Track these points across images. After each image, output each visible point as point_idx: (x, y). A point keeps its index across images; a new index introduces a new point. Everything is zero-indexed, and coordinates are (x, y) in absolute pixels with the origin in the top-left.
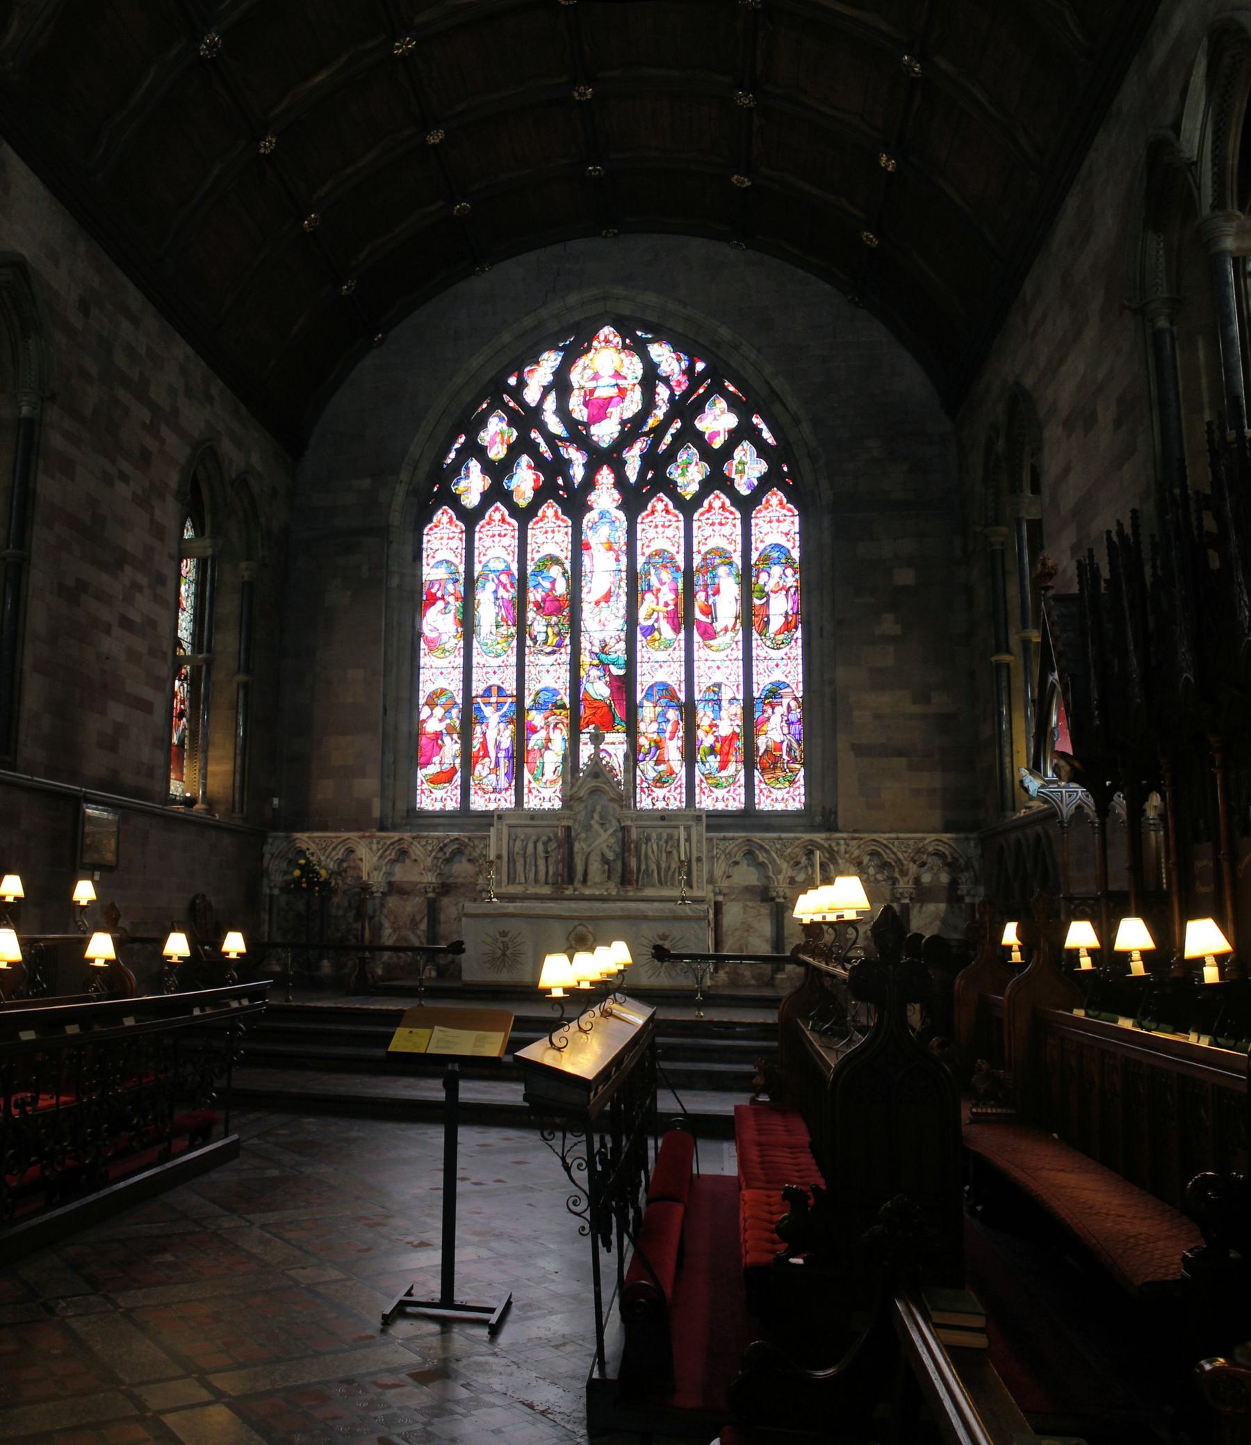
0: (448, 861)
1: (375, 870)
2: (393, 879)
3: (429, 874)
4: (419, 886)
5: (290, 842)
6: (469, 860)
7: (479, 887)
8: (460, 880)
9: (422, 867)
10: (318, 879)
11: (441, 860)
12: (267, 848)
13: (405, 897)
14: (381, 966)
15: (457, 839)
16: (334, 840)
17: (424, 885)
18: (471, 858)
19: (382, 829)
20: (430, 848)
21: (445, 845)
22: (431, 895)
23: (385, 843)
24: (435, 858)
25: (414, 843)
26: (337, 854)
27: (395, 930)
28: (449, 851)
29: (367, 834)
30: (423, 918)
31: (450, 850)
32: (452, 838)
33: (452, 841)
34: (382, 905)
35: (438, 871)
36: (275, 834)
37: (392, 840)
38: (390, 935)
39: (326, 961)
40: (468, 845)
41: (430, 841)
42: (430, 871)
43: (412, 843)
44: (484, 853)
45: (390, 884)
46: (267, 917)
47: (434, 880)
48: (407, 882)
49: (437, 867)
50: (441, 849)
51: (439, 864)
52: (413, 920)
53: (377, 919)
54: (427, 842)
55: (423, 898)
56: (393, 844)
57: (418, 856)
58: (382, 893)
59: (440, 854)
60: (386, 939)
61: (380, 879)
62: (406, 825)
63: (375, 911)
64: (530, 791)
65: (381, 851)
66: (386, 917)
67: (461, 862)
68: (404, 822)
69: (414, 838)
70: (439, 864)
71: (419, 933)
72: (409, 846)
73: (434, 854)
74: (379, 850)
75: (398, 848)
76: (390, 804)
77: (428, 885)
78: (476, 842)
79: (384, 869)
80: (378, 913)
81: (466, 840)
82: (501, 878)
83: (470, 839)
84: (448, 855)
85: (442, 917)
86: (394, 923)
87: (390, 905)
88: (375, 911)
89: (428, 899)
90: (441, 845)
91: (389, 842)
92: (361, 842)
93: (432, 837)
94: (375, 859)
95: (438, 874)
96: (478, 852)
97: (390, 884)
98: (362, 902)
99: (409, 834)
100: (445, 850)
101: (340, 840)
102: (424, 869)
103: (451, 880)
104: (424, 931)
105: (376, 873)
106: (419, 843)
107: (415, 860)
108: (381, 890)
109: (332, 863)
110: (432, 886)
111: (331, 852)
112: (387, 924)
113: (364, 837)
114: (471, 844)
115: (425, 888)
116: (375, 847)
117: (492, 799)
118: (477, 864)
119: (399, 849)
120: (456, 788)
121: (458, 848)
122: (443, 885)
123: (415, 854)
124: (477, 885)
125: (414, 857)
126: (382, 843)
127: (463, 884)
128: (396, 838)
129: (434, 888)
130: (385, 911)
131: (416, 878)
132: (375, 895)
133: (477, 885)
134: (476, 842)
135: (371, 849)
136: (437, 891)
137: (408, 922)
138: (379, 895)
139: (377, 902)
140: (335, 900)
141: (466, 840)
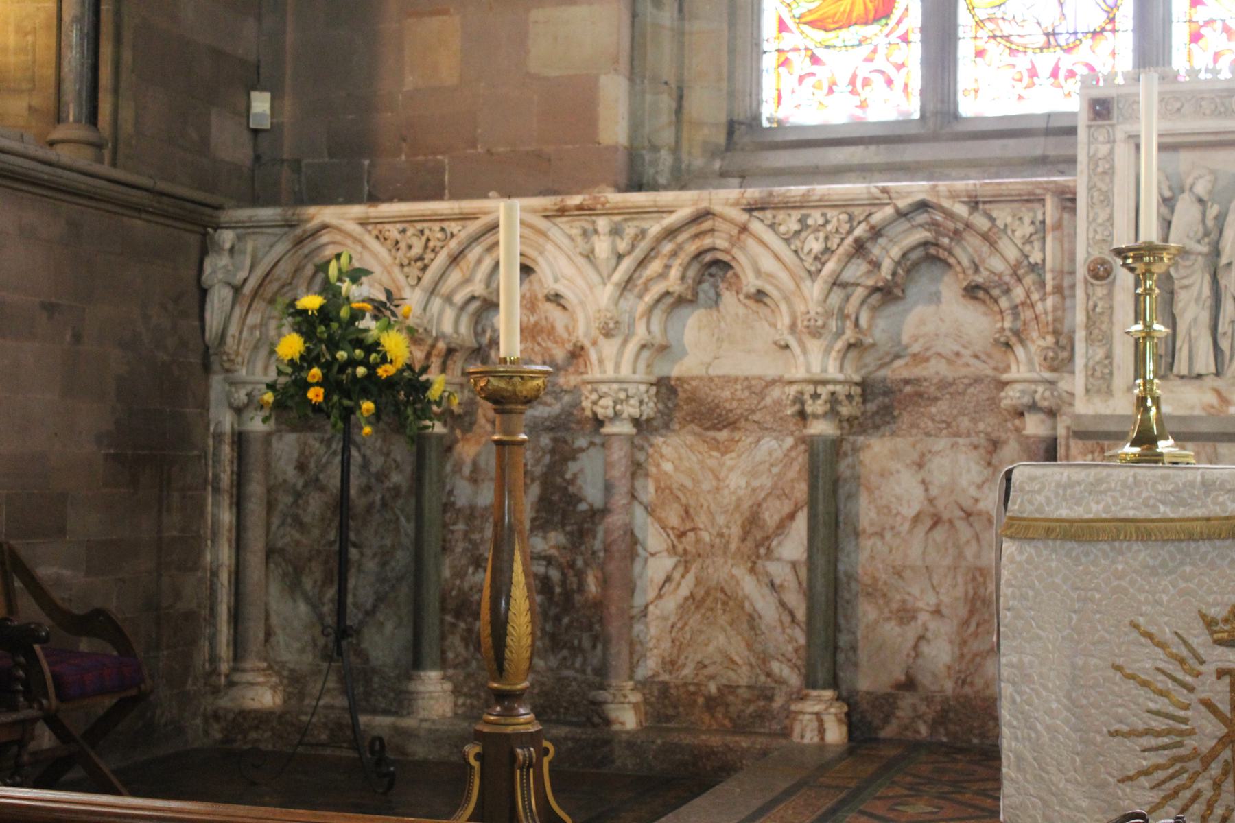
0: (887, 294)
1: (608, 334)
2: (676, 371)
3: (815, 347)
4: (776, 393)
5: (299, 242)
6: (972, 292)
7: (1012, 396)
8: (936, 369)
9: (787, 320)
10: (372, 368)
11: (860, 292)
12: (216, 267)
13: (723, 435)
14: (635, 697)
15: (923, 206)
16: (453, 227)
17: (792, 390)
18: (979, 279)
19: (637, 185)
20: (815, 245)
21: (876, 233)
22: (821, 428)
23: (643, 233)
24: (836, 283)
25: (756, 226)
26: (467, 281)
27: (685, 561)
28: (888, 254)
29: (576, 200)
30: (792, 516)
31: (896, 252)
32: (902, 204)
33: (901, 214)
34: (637, 469)
35: (849, 335)
36: (244, 214)
37: (669, 220)
38: (668, 579)
39: (434, 675)
40: (968, 226)
41: (815, 218)
42: (816, 333)
43: (744, 229)
44: (1035, 257)
45: (665, 388)
46: (227, 517)
47: (833, 372)
48: (729, 380)
49: (843, 316)
50: (860, 248)
51: (851, 308)
52: (752, 521)
53: (615, 520)
54: (802, 221)
55: (790, 441)
56: (670, 233)
57: (770, 276)
58: (636, 422)
59: (856, 270)
60: (652, 594)
61: (625, 371)
62: (723, 174)
63: (608, 488)
64: (1196, 37)
65: (627, 264)
66: (650, 510)
67: (935, 298)
68: (717, 165)
69: (750, 209)
70: (851, 308)
71: (779, 571)
72: (735, 241)
73: (831, 266)
74: (620, 257)
75: (692, 248)
76: (666, 102)
77: (810, 389)
78: (1003, 215)
79: (641, 329)
80: (620, 499)
81: (961, 210)
82: (1109, 356)
83: (974, 203)
84: (887, 267)
85: (866, 512)
86: (682, 534)
87: (667, 467)
88: (608, 488)
89: (810, 443)
90: (860, 231)
91: (655, 228)
92: (554, 233)
93: (825, 204)
94: (606, 294)
95: (850, 346)
96: (1012, 254)
97: (665, 388)
98: (563, 454)
99: (733, 193)
100: (876, 251)
101: (473, 227)
102: (793, 328)
103: (899, 370)
104: (794, 565)
105: (609, 348)
106: (772, 226)
107: (759, 296)
108: (631, 410)
109: (449, 314)
110: (824, 391)
111: (443, 275)
112: (653, 538)
113: (562, 211)
114: (981, 222)
115: (799, 399)
116: (602, 246)
117: (1044, 69)
118: (1004, 303)
119: (698, 255)
120: (905, 39)
121: (925, 244)
122: (866, 388)
123: (758, 273)
124: (1004, 385)
125: (751, 282)
126: (630, 230)
127: (944, 385)
128: (683, 213)
129: (833, 398)
130: (648, 491)
131: (762, 366)
132: (607, 429)
133: (1004, 385)
134: (1003, 215)
135: (589, 256)
136: (845, 410)
137: (735, 531)
138: (627, 428)
139: (618, 453)
140: (467, 450)
141: (961, 210)
